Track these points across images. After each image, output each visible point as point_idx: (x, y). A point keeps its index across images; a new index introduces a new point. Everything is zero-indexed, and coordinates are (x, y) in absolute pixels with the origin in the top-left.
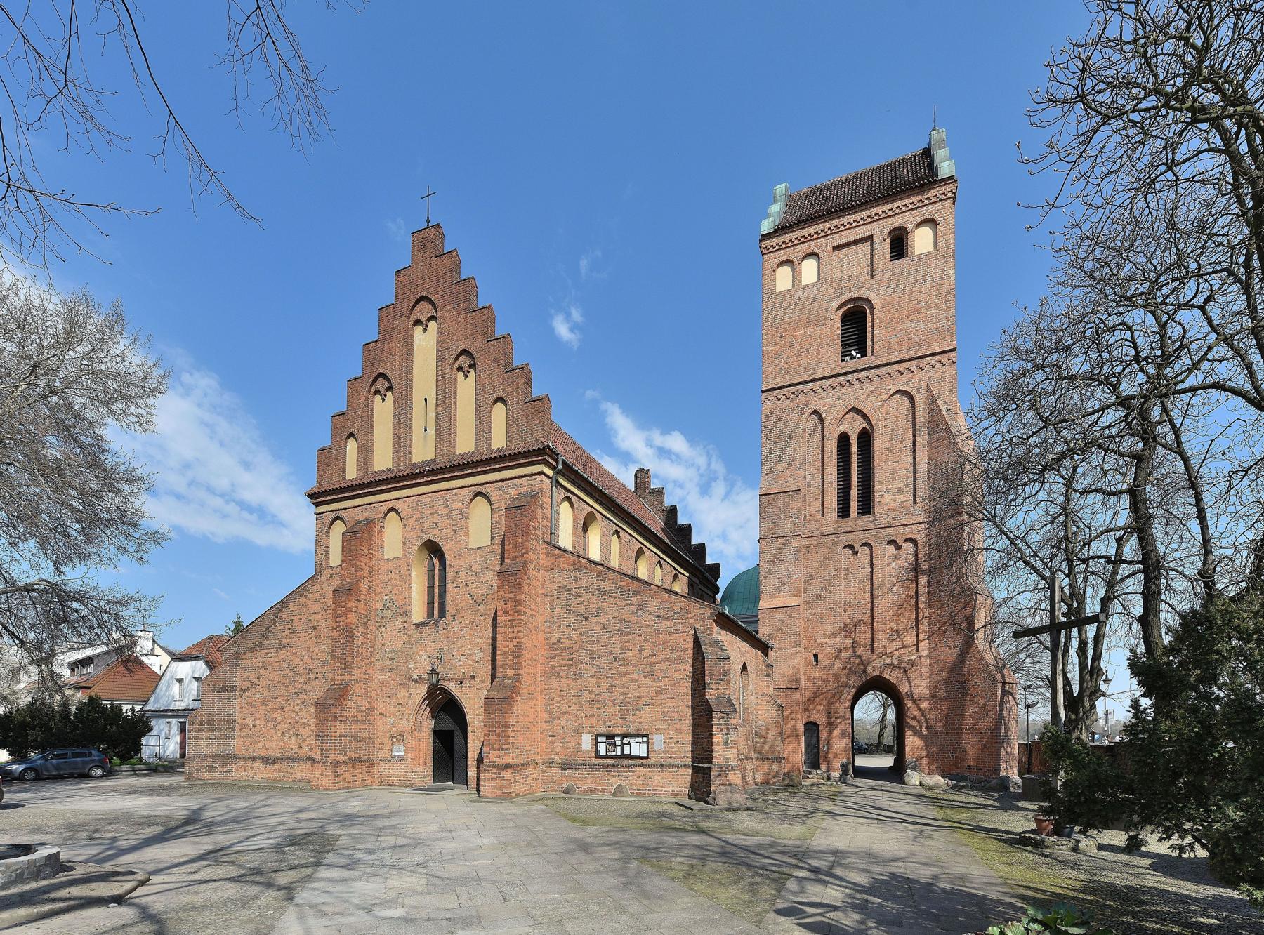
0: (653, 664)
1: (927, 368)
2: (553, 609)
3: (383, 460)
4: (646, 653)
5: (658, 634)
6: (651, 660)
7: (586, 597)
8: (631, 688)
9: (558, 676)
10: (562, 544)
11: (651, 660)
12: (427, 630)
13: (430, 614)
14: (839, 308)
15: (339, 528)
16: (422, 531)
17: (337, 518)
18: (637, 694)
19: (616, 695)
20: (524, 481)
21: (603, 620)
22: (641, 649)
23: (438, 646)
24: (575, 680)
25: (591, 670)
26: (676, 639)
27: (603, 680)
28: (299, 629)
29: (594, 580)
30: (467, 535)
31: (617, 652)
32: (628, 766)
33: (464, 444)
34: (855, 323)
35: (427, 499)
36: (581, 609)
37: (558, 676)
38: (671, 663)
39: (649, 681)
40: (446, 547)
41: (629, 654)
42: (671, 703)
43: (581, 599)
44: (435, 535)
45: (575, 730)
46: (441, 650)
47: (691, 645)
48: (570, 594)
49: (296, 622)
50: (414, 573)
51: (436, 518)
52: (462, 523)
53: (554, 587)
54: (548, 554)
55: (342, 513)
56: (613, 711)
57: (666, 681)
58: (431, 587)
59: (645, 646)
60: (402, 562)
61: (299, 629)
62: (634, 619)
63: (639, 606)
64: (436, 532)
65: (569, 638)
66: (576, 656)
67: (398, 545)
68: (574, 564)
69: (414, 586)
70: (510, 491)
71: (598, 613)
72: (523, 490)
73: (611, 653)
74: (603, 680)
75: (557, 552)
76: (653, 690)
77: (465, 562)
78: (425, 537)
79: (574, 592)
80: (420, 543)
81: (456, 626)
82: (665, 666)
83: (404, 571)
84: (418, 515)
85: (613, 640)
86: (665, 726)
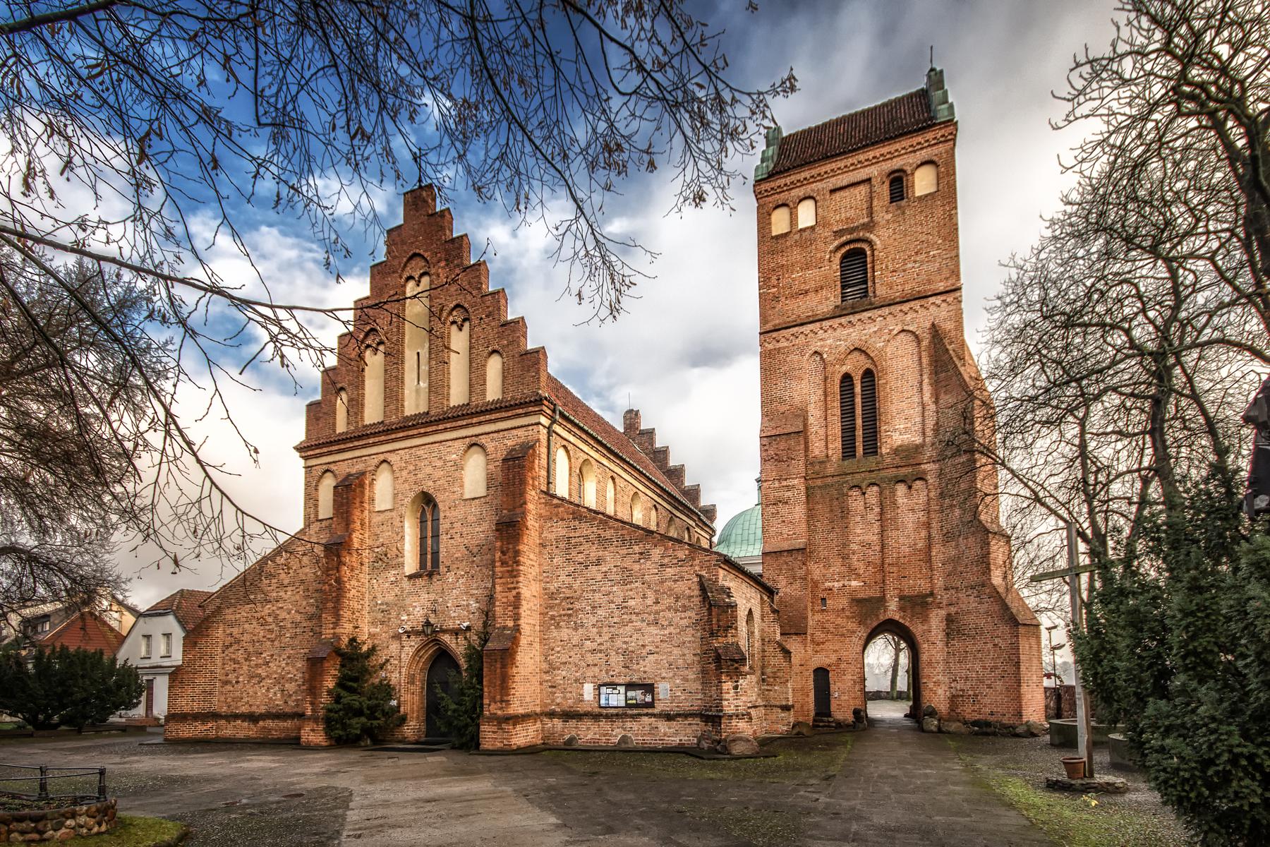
0: (657, 613)
1: (933, 309)
2: (552, 559)
3: (373, 412)
4: (649, 602)
5: (662, 582)
6: (655, 608)
7: (586, 546)
8: (635, 636)
9: (558, 626)
11: (655, 608)
12: (420, 582)
13: (423, 563)
14: (838, 248)
15: (328, 483)
16: (415, 483)
17: (328, 471)
19: (619, 643)
20: (520, 432)
21: (604, 569)
22: (644, 597)
23: (432, 596)
24: (576, 629)
25: (593, 620)
26: (681, 587)
27: (605, 630)
30: (462, 486)
31: (619, 600)
32: (632, 716)
33: (457, 395)
34: (855, 261)
35: (420, 452)
36: (580, 558)
37: (558, 626)
38: (676, 611)
39: (653, 630)
40: (439, 498)
41: (632, 603)
42: (676, 651)
43: (582, 548)
44: (429, 486)
45: (576, 681)
46: (435, 601)
47: (697, 592)
48: (569, 544)
50: (407, 525)
51: (429, 470)
52: (457, 474)
53: (552, 536)
55: (332, 467)
56: (616, 660)
57: (671, 629)
58: (423, 539)
59: (649, 593)
60: (394, 514)
62: (636, 567)
63: (641, 554)
64: (430, 483)
65: (570, 587)
66: (577, 606)
67: (389, 497)
69: (407, 538)
71: (598, 562)
72: (520, 441)
73: (612, 602)
74: (605, 630)
75: (555, 501)
76: (658, 639)
77: (458, 514)
78: (418, 489)
80: (412, 495)
81: (451, 578)
82: (669, 614)
83: (397, 523)
84: (412, 468)
85: (615, 589)
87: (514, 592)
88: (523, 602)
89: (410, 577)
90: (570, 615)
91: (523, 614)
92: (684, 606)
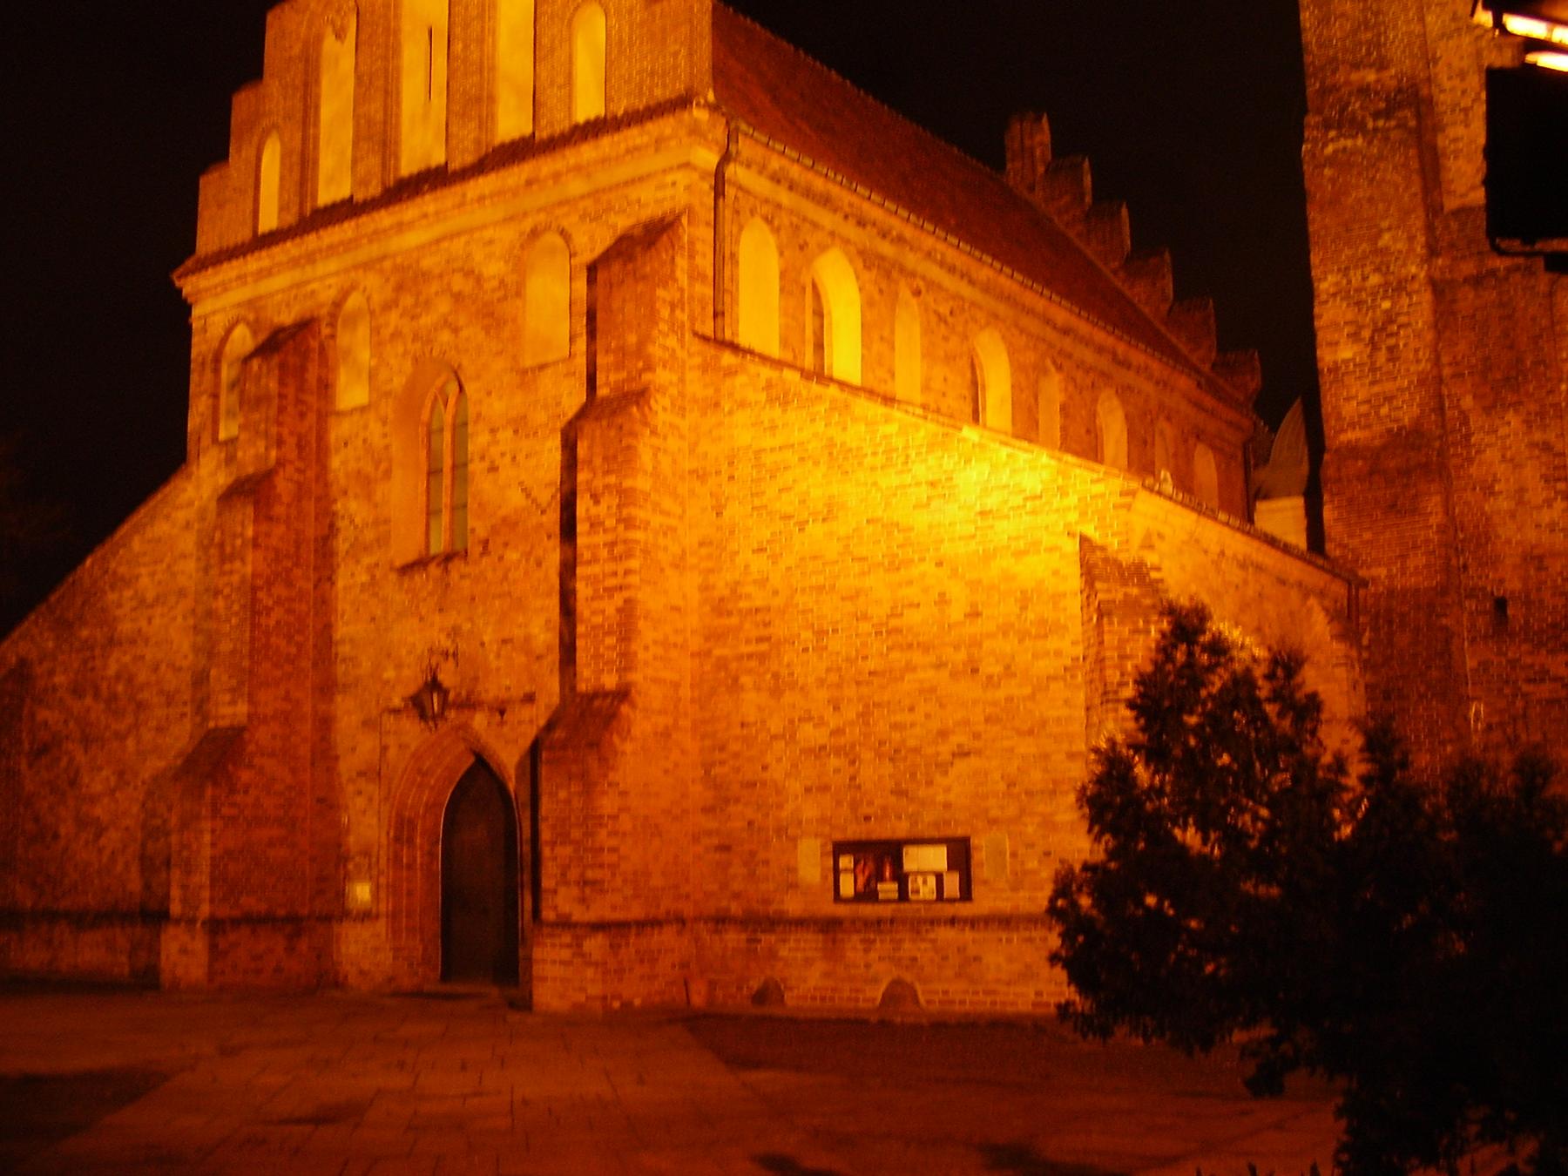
0: (975, 643)
8: (922, 708)
10: (744, 340)
18: (935, 725)
21: (842, 531)
28: (150, 596)
29: (820, 426)
42: (1026, 747)
49: (145, 581)
54: (705, 368)
61: (150, 596)
68: (769, 386)
70: (613, 219)
75: (728, 358)
79: (768, 459)
86: (1012, 811)
87: (618, 599)
88: (641, 624)
89: (407, 569)
90: (762, 658)
91: (641, 655)
92: (1042, 622)
